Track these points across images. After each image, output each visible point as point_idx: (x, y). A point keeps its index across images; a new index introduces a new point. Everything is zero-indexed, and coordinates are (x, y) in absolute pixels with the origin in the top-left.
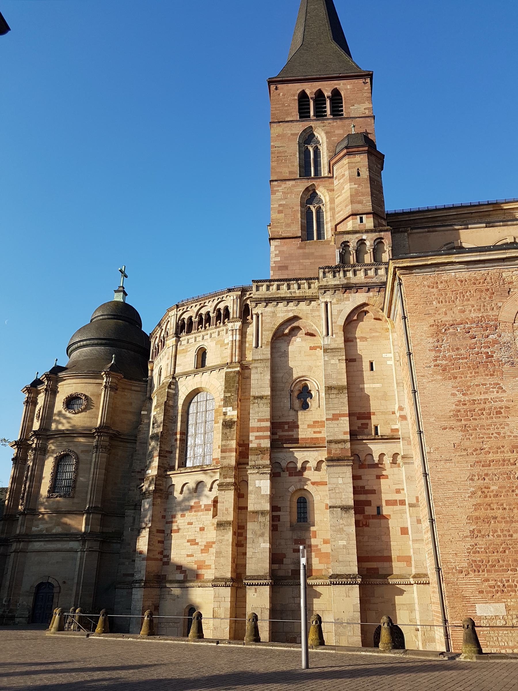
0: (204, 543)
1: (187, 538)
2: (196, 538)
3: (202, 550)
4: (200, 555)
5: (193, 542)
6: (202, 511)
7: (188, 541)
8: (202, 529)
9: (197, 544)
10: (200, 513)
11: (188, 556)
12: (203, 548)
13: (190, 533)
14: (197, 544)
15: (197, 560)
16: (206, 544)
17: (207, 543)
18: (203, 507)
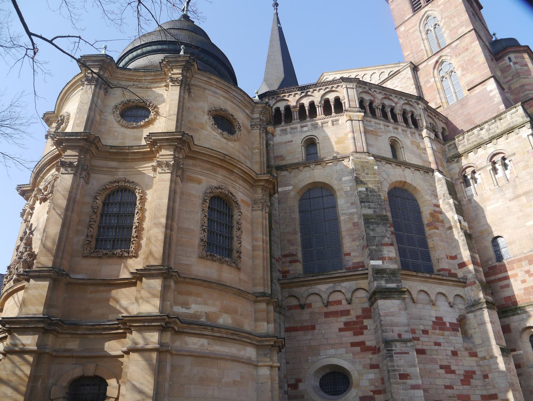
0: (462, 372)
1: (439, 363)
2: (450, 364)
3: (462, 380)
4: (461, 387)
5: (448, 369)
6: (448, 330)
7: (442, 367)
8: (455, 353)
9: (453, 372)
10: (446, 333)
11: (447, 387)
12: (462, 378)
13: (440, 357)
14: (453, 372)
15: (458, 393)
16: (464, 373)
17: (466, 371)
18: (448, 325)
